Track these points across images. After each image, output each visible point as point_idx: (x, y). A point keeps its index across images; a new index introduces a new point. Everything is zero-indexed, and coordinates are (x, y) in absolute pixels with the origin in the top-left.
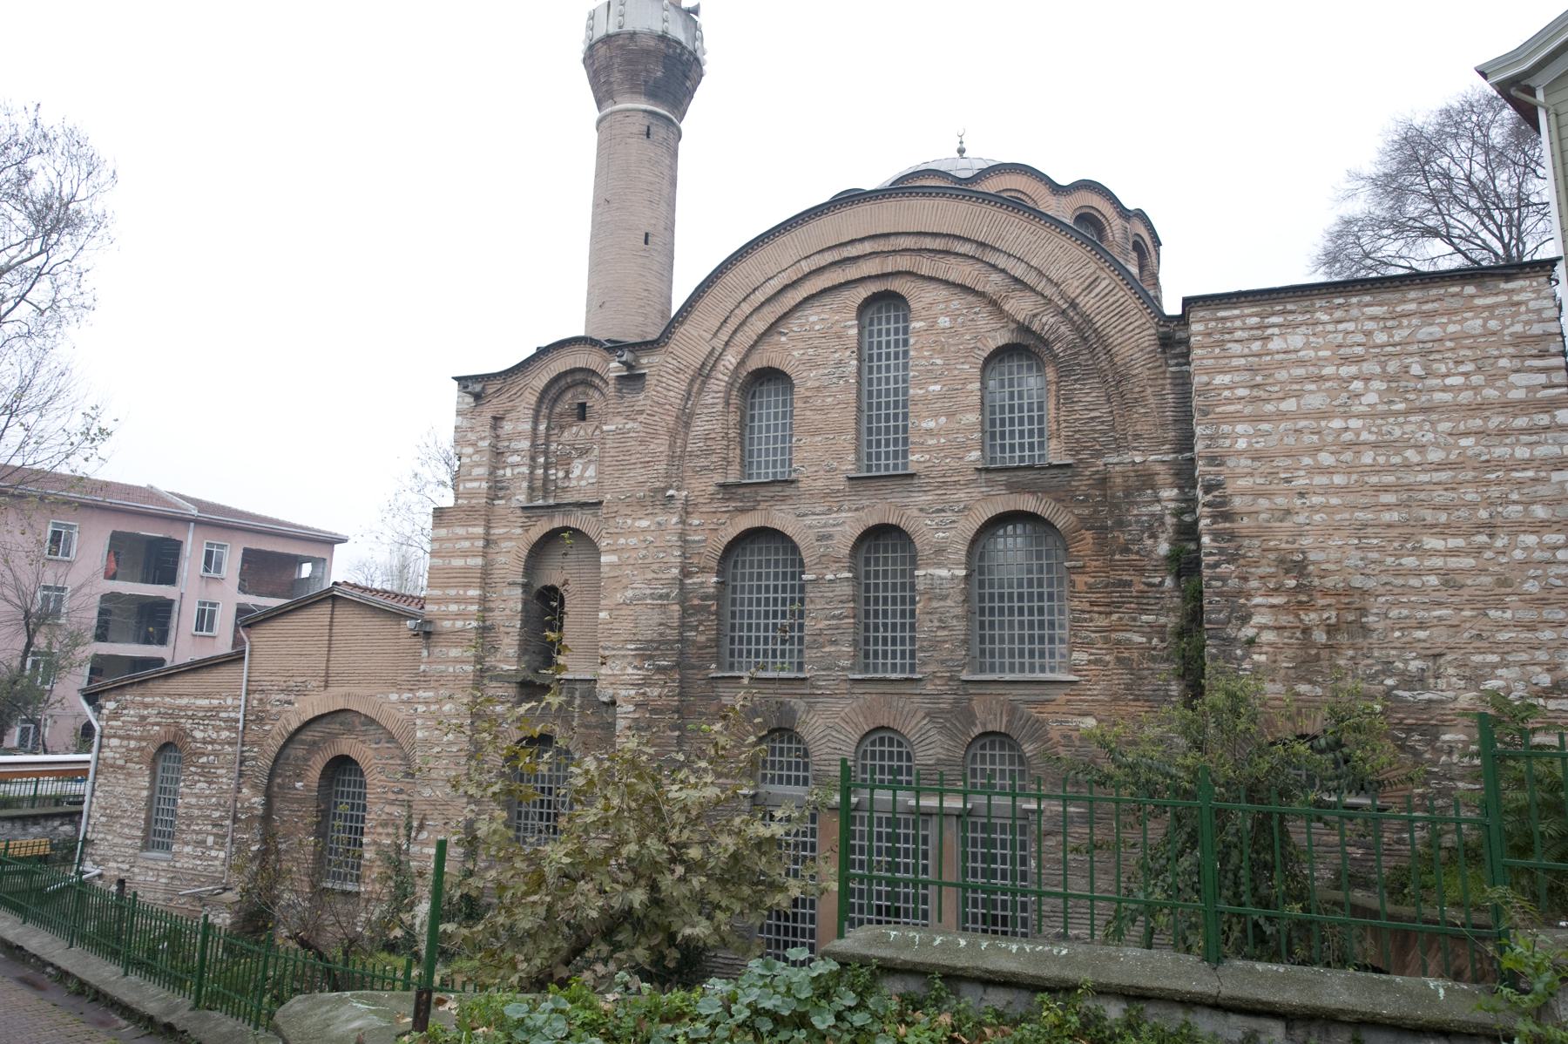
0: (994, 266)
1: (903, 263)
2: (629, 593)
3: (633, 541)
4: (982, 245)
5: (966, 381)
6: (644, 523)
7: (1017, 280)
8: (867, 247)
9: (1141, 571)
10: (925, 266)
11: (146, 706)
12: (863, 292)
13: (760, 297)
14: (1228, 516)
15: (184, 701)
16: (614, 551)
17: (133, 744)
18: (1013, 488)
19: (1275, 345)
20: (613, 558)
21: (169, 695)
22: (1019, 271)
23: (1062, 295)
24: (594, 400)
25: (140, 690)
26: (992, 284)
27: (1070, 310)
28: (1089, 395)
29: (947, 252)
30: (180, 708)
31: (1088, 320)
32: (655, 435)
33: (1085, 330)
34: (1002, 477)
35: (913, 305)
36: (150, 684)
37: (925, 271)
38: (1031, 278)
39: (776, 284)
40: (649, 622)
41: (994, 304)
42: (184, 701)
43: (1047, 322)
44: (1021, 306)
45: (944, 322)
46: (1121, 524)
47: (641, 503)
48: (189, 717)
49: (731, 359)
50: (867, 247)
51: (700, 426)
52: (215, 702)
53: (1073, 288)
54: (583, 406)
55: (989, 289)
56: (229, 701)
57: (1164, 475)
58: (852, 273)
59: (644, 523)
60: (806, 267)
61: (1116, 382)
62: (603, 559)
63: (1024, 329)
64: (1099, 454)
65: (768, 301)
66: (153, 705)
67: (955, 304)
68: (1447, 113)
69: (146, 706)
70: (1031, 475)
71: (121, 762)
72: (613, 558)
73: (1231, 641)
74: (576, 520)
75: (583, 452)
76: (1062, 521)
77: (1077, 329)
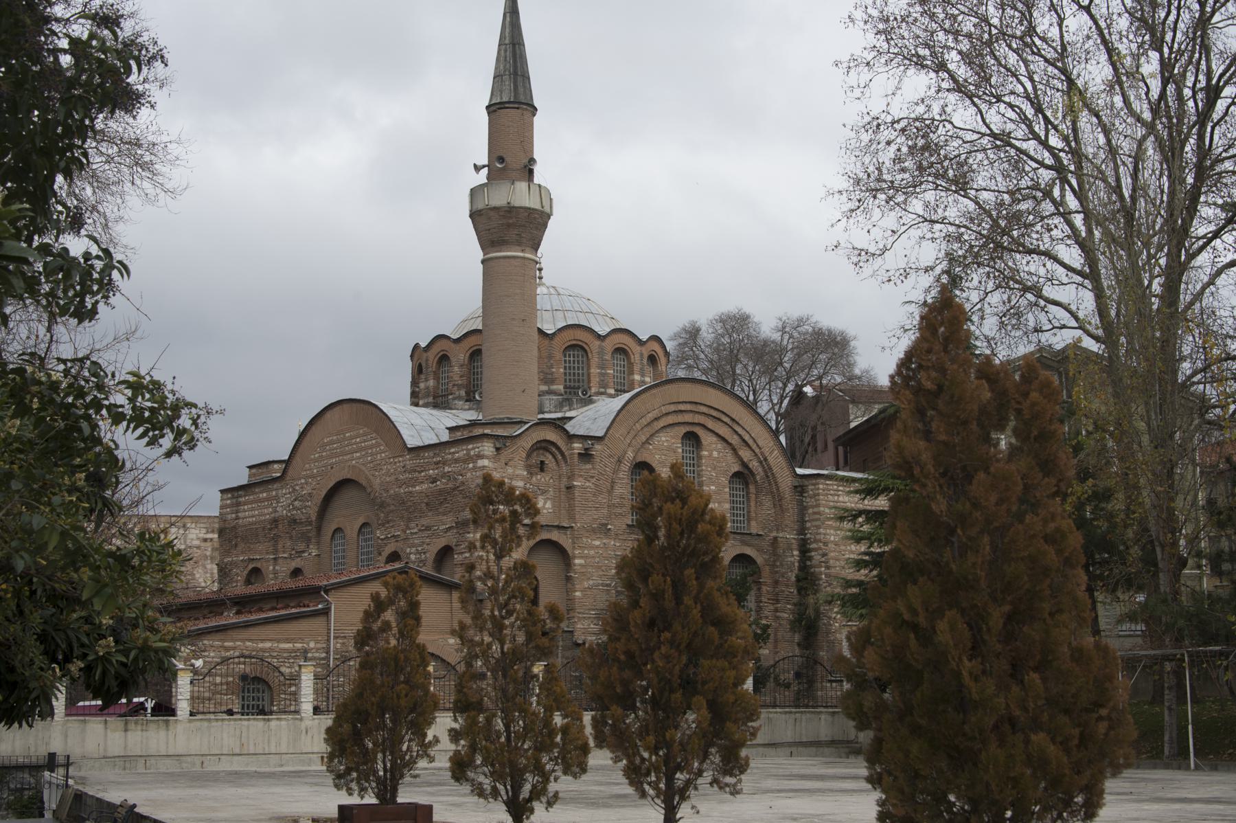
0: (736, 432)
1: (701, 419)
2: (591, 582)
3: (592, 552)
4: (733, 420)
5: (724, 487)
6: (597, 543)
7: (744, 441)
8: (688, 407)
9: (787, 586)
10: (710, 424)
11: (227, 649)
12: (684, 430)
13: (644, 421)
14: (828, 568)
15: (268, 645)
16: (581, 557)
17: (218, 680)
18: (744, 543)
19: (841, 499)
20: (582, 561)
21: (250, 640)
22: (747, 438)
23: (762, 453)
24: (549, 459)
25: (219, 636)
26: (734, 440)
27: (764, 461)
28: (767, 503)
29: (719, 419)
30: (264, 650)
31: (770, 469)
32: (601, 492)
33: (768, 470)
34: (738, 537)
35: (704, 442)
36: (230, 632)
37: (710, 426)
38: (751, 442)
39: (651, 416)
40: (602, 601)
41: (734, 450)
42: (268, 645)
43: (754, 465)
44: (745, 454)
45: (715, 454)
46: (782, 565)
47: (594, 530)
48: (274, 657)
49: (630, 454)
50: (688, 407)
51: (618, 490)
52: (299, 645)
53: (766, 451)
54: (542, 462)
55: (733, 442)
56: (312, 645)
57: (795, 544)
58: (680, 418)
59: (597, 543)
60: (664, 410)
61: (778, 500)
62: (577, 561)
63: (744, 465)
64: (771, 531)
65: (649, 424)
66: (234, 648)
67: (719, 446)
68: (736, 323)
69: (227, 649)
70: (749, 538)
71: (207, 695)
72: (582, 561)
73: (830, 618)
74: (554, 536)
75: (544, 492)
76: (759, 560)
77: (765, 471)
